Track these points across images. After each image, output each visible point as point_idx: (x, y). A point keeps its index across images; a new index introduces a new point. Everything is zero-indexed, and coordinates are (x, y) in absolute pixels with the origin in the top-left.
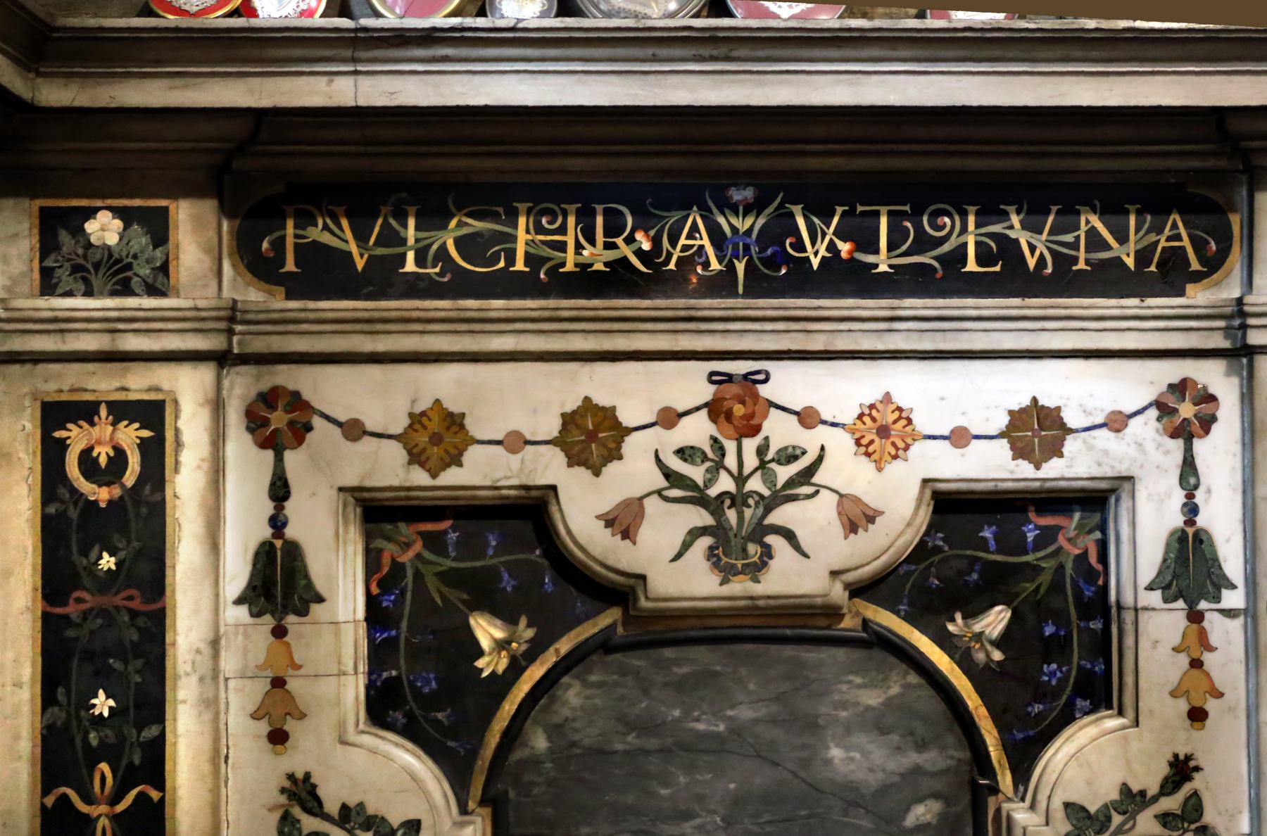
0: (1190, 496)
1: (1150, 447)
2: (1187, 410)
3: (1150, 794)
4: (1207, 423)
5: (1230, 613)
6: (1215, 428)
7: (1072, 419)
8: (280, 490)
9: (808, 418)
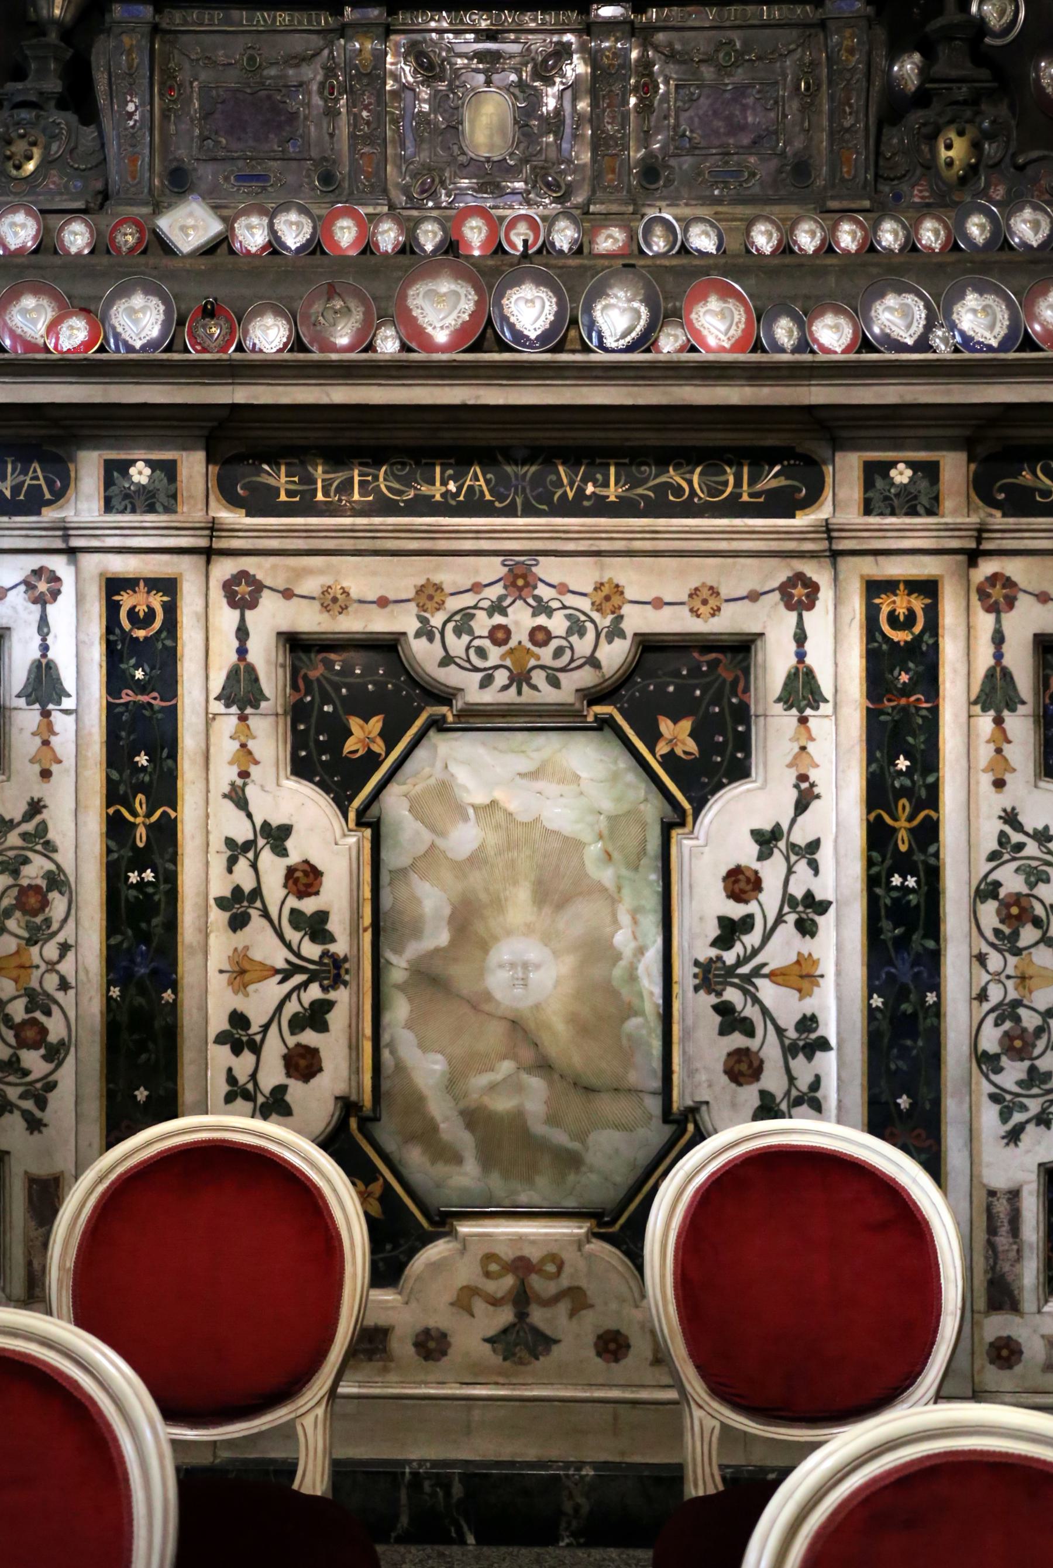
0: (44, 640)
1: (20, 608)
2: (43, 586)
3: (16, 821)
4: (55, 594)
5: (66, 712)
6: (60, 598)
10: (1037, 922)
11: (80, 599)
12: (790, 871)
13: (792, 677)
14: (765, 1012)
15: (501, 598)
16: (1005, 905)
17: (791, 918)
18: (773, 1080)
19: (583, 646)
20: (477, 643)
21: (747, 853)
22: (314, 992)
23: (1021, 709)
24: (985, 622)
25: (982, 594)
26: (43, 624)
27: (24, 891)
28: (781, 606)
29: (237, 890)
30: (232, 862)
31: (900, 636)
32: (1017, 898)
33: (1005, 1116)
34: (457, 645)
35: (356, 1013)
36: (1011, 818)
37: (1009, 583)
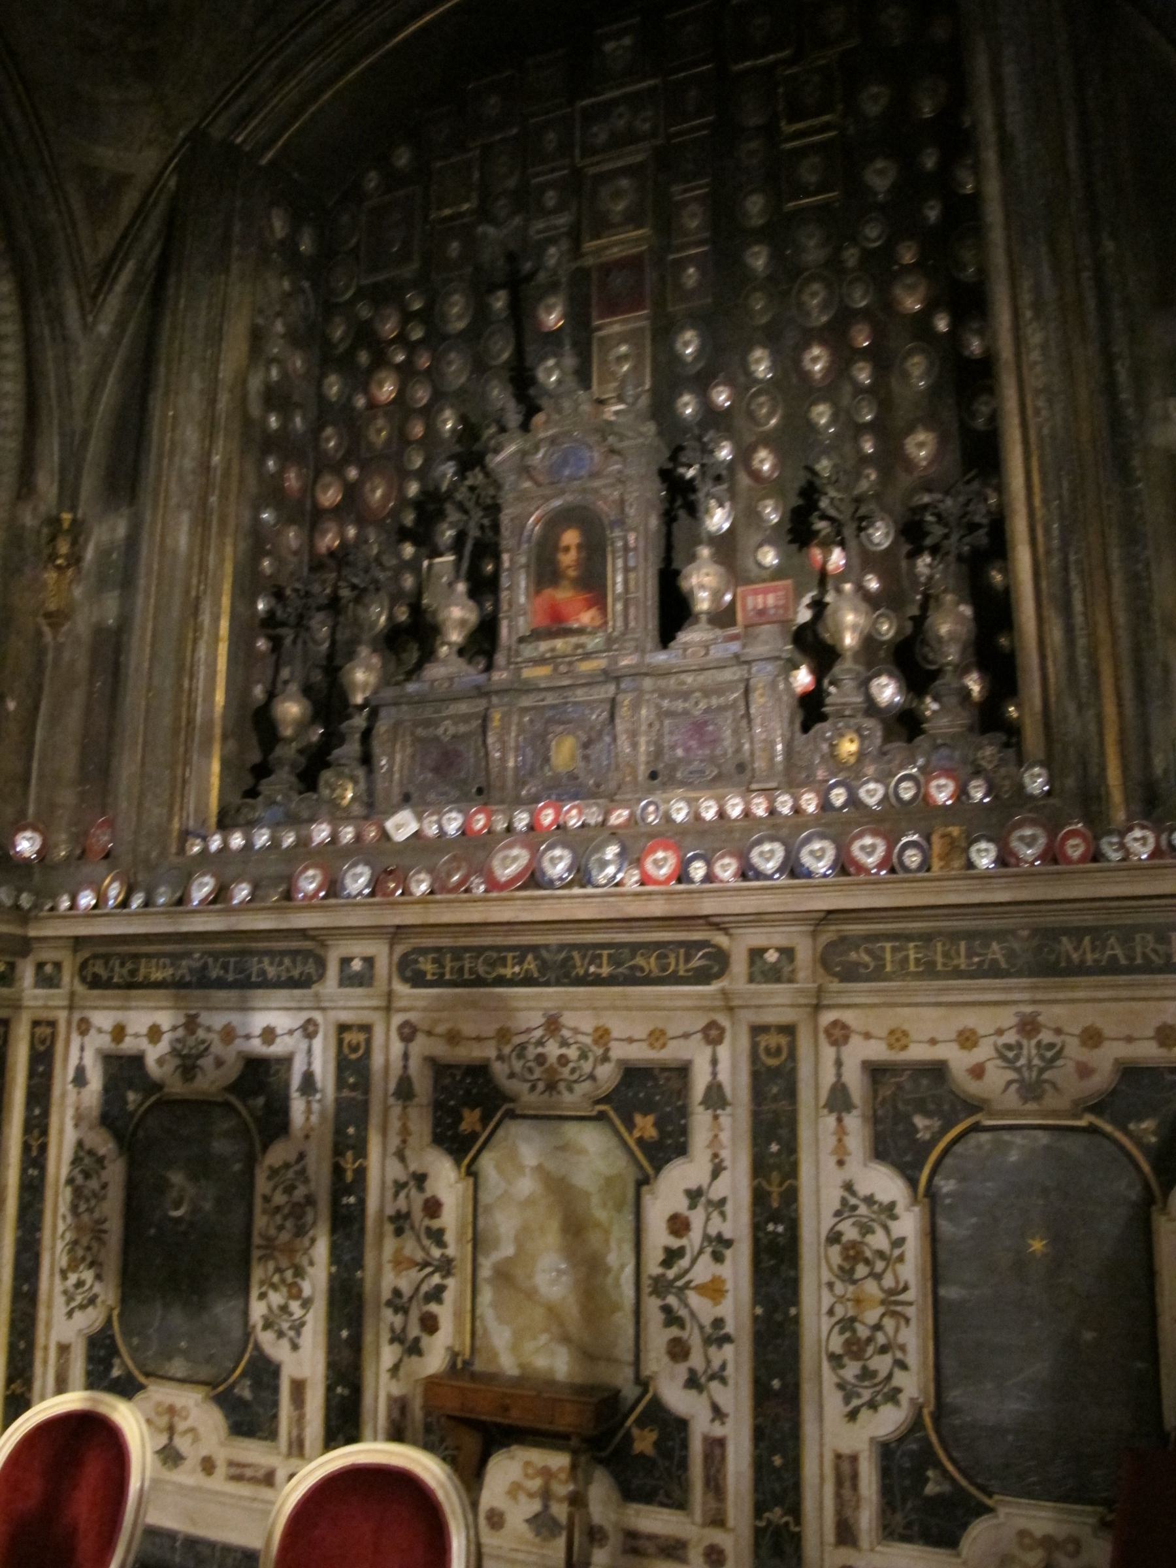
7: (279, 1031)
8: (82, 1049)
9: (209, 1029)
10: (867, 1262)
11: (325, 1037)
12: (708, 1219)
13: (709, 1088)
14: (693, 1314)
15: (542, 1037)
16: (846, 1249)
17: (709, 1250)
18: (696, 1360)
19: (587, 1067)
20: (529, 1064)
21: (680, 1204)
22: (436, 1279)
23: (855, 1112)
24: (828, 1053)
25: (828, 1033)
26: (309, 1051)
27: (296, 1205)
28: (703, 1043)
29: (398, 1213)
30: (396, 1195)
31: (772, 1062)
32: (854, 1245)
33: (847, 1400)
34: (518, 1065)
35: (461, 1293)
36: (849, 1187)
37: (845, 1027)
